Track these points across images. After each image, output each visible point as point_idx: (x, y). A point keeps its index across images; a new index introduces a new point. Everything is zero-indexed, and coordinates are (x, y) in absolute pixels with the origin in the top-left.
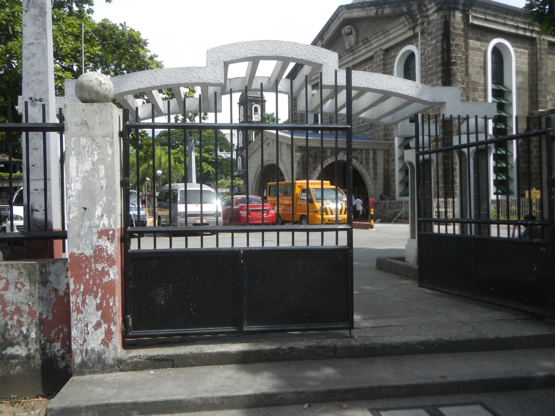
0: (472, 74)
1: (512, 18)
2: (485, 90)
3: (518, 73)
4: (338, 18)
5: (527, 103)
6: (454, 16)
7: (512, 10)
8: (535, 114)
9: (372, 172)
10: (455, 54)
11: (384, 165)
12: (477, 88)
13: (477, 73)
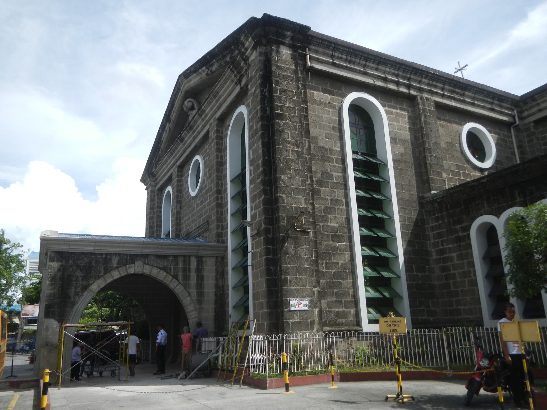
0: (320, 138)
1: (375, 66)
2: (344, 161)
3: (393, 140)
4: (180, 92)
5: (414, 183)
6: (278, 52)
7: (373, 55)
8: (427, 197)
9: (194, 291)
10: (281, 103)
11: (217, 279)
12: (329, 158)
13: (328, 136)
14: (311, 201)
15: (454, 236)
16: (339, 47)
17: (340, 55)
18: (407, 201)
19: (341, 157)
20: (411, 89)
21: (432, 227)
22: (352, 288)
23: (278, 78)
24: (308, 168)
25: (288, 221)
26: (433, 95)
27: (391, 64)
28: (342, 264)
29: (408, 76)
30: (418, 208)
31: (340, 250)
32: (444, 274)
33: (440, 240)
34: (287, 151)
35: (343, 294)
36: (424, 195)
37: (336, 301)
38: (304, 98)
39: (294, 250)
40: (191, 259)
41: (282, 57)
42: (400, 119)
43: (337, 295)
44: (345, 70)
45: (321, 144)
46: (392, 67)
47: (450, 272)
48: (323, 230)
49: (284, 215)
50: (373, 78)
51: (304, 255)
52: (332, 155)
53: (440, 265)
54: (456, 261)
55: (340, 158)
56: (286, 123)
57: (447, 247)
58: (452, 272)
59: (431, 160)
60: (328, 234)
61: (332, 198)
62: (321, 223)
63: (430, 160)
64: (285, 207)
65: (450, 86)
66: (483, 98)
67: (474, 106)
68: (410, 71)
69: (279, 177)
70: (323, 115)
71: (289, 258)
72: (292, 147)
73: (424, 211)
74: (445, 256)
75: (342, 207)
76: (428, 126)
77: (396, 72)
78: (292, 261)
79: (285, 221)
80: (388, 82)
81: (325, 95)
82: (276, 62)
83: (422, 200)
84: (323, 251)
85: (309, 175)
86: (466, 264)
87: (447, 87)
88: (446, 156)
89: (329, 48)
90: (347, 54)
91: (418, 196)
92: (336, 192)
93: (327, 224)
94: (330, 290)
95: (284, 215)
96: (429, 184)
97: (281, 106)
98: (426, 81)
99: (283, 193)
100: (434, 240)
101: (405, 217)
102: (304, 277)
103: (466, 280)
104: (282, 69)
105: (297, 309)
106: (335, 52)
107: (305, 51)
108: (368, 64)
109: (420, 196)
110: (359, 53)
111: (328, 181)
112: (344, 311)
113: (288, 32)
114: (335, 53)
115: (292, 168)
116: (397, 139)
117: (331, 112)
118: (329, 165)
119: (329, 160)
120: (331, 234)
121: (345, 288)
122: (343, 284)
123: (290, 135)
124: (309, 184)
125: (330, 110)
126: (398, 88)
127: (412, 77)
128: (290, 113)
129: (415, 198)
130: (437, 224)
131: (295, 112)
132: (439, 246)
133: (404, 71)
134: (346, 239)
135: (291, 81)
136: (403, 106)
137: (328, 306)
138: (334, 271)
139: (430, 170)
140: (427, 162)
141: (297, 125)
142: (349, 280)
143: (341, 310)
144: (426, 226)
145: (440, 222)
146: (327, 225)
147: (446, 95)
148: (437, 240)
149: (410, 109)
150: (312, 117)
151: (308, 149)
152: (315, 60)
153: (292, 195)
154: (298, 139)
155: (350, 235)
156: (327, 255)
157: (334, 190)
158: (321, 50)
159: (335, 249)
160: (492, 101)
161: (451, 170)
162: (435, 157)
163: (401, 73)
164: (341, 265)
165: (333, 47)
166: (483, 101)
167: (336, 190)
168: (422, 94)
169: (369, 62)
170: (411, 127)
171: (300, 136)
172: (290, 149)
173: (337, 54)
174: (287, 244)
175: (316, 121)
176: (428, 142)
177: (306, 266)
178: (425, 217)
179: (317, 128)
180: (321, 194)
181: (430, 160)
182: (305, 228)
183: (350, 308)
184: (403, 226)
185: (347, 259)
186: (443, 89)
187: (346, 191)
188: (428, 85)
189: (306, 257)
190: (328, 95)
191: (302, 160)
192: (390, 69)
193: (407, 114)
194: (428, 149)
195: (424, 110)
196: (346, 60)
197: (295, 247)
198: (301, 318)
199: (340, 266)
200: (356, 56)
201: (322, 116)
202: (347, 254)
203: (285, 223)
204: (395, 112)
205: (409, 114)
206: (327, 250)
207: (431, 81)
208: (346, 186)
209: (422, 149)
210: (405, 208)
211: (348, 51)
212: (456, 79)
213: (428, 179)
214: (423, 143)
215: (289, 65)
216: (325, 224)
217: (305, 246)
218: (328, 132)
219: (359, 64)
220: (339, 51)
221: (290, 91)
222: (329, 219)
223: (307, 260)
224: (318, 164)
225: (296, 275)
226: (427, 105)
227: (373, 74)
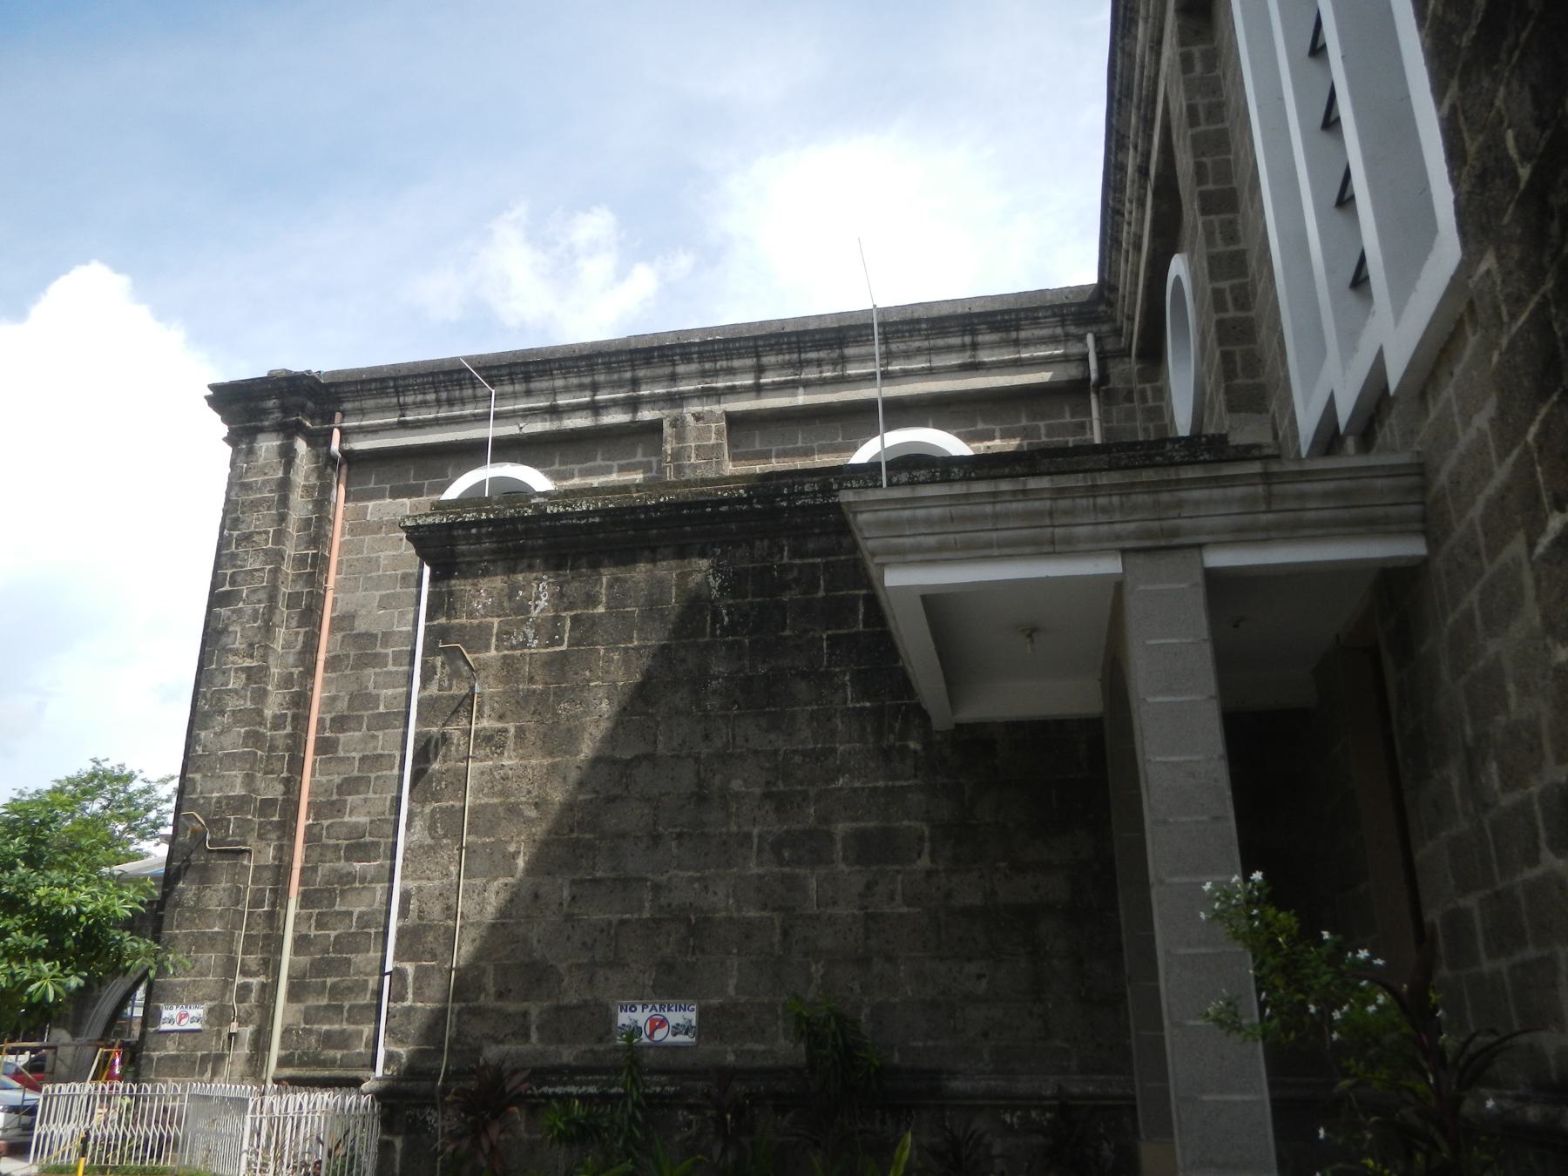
1: (519, 387)
10: (234, 566)
12: (376, 655)
16: (407, 382)
17: (420, 398)
22: (377, 972)
24: (293, 697)
27: (560, 368)
29: (628, 375)
35: (350, 989)
37: (327, 1007)
41: (257, 461)
43: (335, 991)
44: (438, 428)
46: (569, 373)
48: (328, 837)
52: (386, 648)
60: (338, 845)
66: (926, 344)
67: (893, 378)
68: (627, 361)
70: (381, 554)
77: (587, 380)
94: (318, 980)
98: (694, 367)
102: (206, 955)
105: (175, 1027)
107: (331, 420)
110: (462, 375)
112: (343, 1032)
119: (378, 661)
121: (359, 972)
122: (355, 963)
123: (239, 635)
127: (641, 373)
133: (608, 367)
137: (305, 1019)
142: (371, 954)
143: (336, 1027)
151: (300, 653)
157: (376, 733)
158: (370, 403)
159: (349, 878)
160: (968, 339)
165: (393, 387)
167: (380, 734)
173: (410, 399)
177: (216, 929)
180: (340, 748)
183: (363, 1023)
189: (219, 909)
190: (406, 500)
191: (255, 686)
196: (439, 403)
198: (182, 1048)
199: (354, 920)
206: (327, 883)
211: (433, 383)
217: (223, 885)
220: (414, 390)
223: (221, 916)
224: (346, 676)
225: (189, 952)
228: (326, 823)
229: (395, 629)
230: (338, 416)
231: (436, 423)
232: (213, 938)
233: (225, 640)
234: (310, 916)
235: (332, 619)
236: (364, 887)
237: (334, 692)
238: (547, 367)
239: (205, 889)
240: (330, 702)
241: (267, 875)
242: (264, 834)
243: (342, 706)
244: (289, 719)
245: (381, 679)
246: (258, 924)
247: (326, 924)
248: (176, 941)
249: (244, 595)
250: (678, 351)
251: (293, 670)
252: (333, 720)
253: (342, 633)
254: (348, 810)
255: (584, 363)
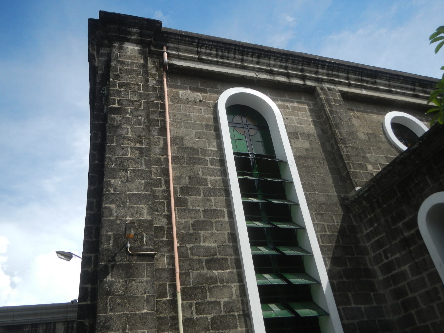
1: (255, 59)
2: (223, 162)
5: (330, 180)
6: (121, 48)
10: (119, 96)
12: (200, 159)
14: (166, 213)
15: (398, 239)
16: (204, 42)
17: (208, 51)
18: (324, 204)
19: (218, 158)
20: (307, 80)
21: (367, 234)
23: (118, 72)
24: (163, 171)
25: (115, 241)
26: (336, 85)
27: (274, 56)
28: (226, 304)
29: (300, 67)
30: (341, 212)
31: (222, 281)
32: (399, 301)
33: (381, 251)
34: (123, 149)
36: (347, 195)
38: (159, 93)
39: (123, 285)
40: (57, 327)
41: (126, 53)
42: (299, 112)
44: (217, 66)
45: (189, 145)
46: (277, 59)
47: (407, 297)
48: (192, 254)
49: (110, 233)
50: (255, 72)
51: (143, 292)
52: (205, 156)
53: (390, 288)
54: (411, 278)
55: (217, 159)
56: (126, 117)
57: (393, 258)
58: (410, 295)
59: (348, 152)
60: (200, 259)
61: (207, 208)
62: (189, 244)
63: (345, 151)
64: (113, 221)
65: (356, 75)
66: (401, 85)
68: (301, 61)
69: (107, 182)
70: (192, 114)
71: (112, 301)
72: (132, 144)
73: (351, 215)
74: (394, 272)
75: (222, 220)
76: (336, 115)
77: (284, 64)
78: (119, 304)
79: (111, 242)
80: (274, 75)
81: (193, 94)
82: (117, 58)
83: (346, 202)
84: (192, 286)
85: (163, 179)
86: (426, 279)
87: (351, 76)
88: (370, 149)
89: (193, 45)
90: (217, 49)
91: (339, 197)
92: (213, 200)
93: (198, 245)
95: (110, 233)
96: (350, 179)
97: (119, 101)
98: (325, 71)
99: (112, 202)
100: (374, 252)
101: (323, 225)
103: (434, 305)
104: (125, 64)
106: (201, 48)
107: (162, 49)
108: (245, 58)
109: (342, 196)
110: (231, 47)
111: (199, 187)
113: (133, 28)
114: (202, 50)
115: (129, 168)
116: (299, 133)
117: (203, 111)
118: (201, 168)
119: (202, 162)
120: (206, 258)
123: (130, 130)
124: (163, 191)
125: (202, 108)
126: (290, 81)
127: (305, 68)
128: (133, 107)
129: (336, 200)
130: (372, 228)
131: (140, 105)
132: (382, 260)
133: (293, 62)
134: (231, 264)
135: (137, 74)
136: (301, 99)
138: (212, 315)
139: (348, 163)
140: (342, 153)
141: (142, 119)
142: (239, 329)
144: (359, 235)
145: (376, 225)
146: (199, 246)
147: (352, 84)
148: (378, 252)
149: (310, 103)
150: (175, 116)
151: (163, 149)
152: (176, 58)
153: (126, 204)
154: (142, 134)
155: (236, 257)
156: (199, 291)
159: (213, 280)
160: (413, 87)
161: (380, 164)
162: (352, 147)
163: (290, 65)
164: (224, 306)
166: (402, 88)
167: (212, 199)
168: (322, 85)
169: (247, 56)
170: (315, 120)
171: (146, 130)
172: (128, 146)
173: (204, 51)
174: (112, 277)
175: (181, 120)
176: (339, 132)
177: (145, 311)
178: (354, 223)
179: (183, 127)
180: (189, 203)
181: (345, 151)
182: (147, 250)
184: (321, 238)
185: (234, 294)
186: (347, 79)
187: (229, 198)
188: (328, 75)
190: (199, 94)
191: (147, 158)
192: (275, 61)
193: (307, 107)
194: (341, 139)
195: (327, 100)
196: (217, 56)
197: (126, 281)
199: (222, 307)
200: (229, 51)
201: (190, 115)
202: (234, 287)
203: (111, 245)
204: (291, 107)
205: (309, 107)
206: (198, 283)
207: (330, 71)
208: (227, 192)
209: (333, 141)
210: (322, 214)
211: (217, 46)
212: (360, 66)
213: (348, 173)
214: (334, 134)
215: (136, 59)
216: (195, 245)
217: (145, 279)
218: (199, 131)
219: (234, 59)
220: (206, 47)
221: (134, 84)
222: (202, 237)
223: (147, 300)
225: (125, 329)
226: (330, 94)
227: (254, 68)
228: (189, 246)
229: (207, 148)
230: (165, 48)
231: (217, 63)
232: (143, 317)
233: (120, 131)
234: (191, 306)
235: (171, 138)
236: (224, 286)
237: (178, 174)
238: (269, 54)
239: (131, 281)
240: (178, 179)
241: (165, 275)
242: (158, 248)
243: (185, 181)
244: (163, 182)
245: (206, 171)
246: (165, 309)
247: (204, 310)
248: (111, 322)
249: (129, 111)
250: (320, 63)
251: (160, 156)
252: (181, 189)
253: (177, 146)
254: (202, 239)
255: (284, 57)
